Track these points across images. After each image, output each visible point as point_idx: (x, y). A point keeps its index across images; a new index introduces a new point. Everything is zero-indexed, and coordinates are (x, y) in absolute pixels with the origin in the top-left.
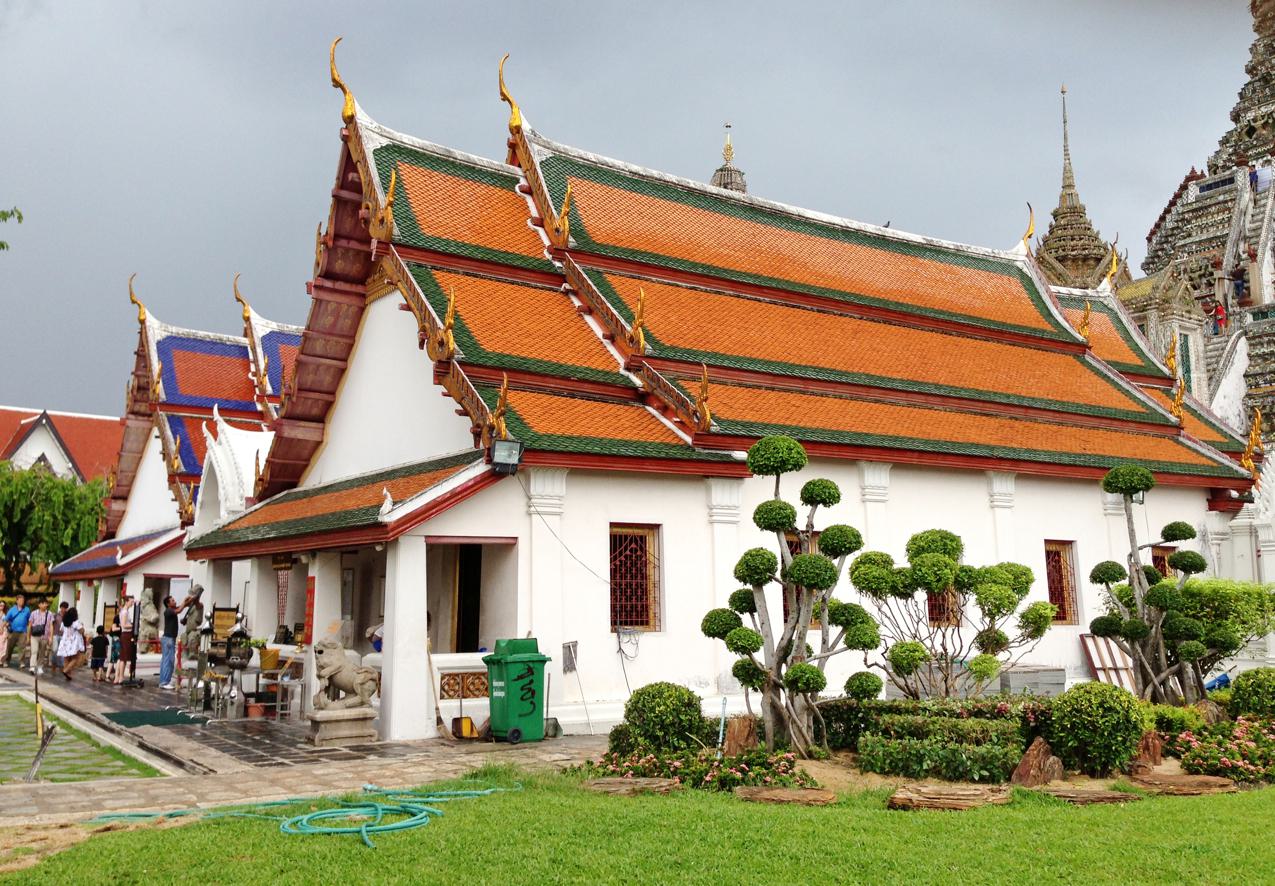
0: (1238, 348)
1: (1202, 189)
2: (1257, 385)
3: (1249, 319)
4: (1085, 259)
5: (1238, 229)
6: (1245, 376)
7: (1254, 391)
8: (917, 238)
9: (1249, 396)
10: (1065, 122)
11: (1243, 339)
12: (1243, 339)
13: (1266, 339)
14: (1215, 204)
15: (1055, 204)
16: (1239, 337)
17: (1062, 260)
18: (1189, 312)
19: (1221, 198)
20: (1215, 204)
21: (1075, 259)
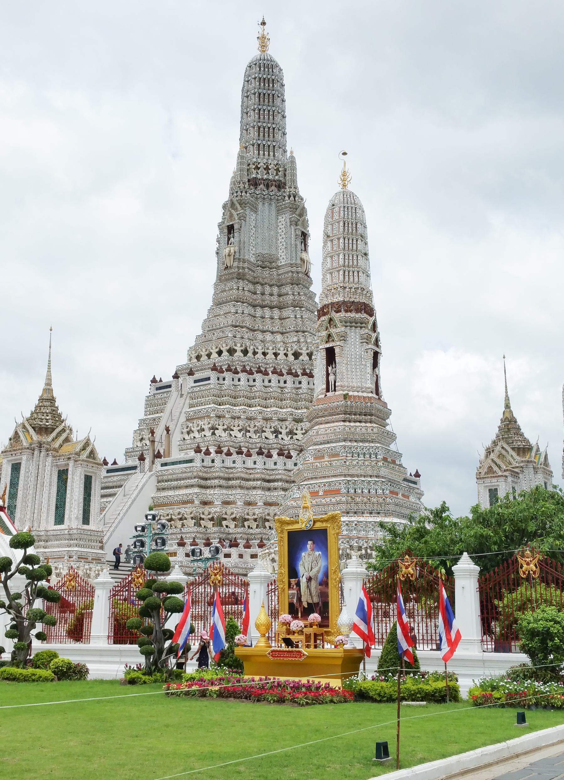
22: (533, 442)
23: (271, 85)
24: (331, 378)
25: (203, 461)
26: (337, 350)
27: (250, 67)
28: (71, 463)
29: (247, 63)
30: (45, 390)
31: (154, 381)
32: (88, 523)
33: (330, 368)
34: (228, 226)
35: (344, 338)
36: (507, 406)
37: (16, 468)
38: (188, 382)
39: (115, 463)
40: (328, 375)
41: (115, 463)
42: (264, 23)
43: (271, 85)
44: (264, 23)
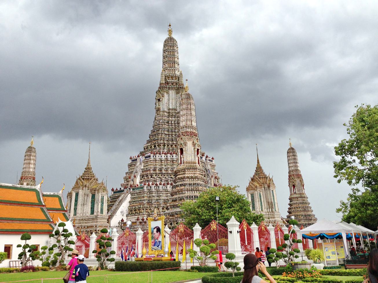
0: (128, 196)
1: (132, 161)
2: (131, 204)
3: (132, 190)
4: (88, 179)
5: (135, 170)
6: (129, 202)
7: (130, 205)
8: (11, 185)
9: (129, 206)
10: (90, 150)
11: (130, 194)
12: (130, 194)
13: (133, 194)
14: (133, 164)
15: (86, 166)
16: (129, 193)
17: (83, 179)
18: (103, 191)
19: (134, 163)
20: (133, 164)
21: (86, 179)
22: (268, 175)
23: (173, 48)
24: (182, 159)
25: (147, 187)
26: (184, 149)
27: (165, 42)
28: (96, 192)
29: (164, 40)
30: (88, 165)
31: (131, 158)
32: (103, 214)
33: (182, 156)
34: (158, 99)
35: (185, 144)
36: (258, 162)
37: (77, 195)
38: (142, 158)
39: (117, 189)
40: (181, 158)
41: (117, 189)
42: (170, 26)
43: (173, 48)
44: (170, 26)
